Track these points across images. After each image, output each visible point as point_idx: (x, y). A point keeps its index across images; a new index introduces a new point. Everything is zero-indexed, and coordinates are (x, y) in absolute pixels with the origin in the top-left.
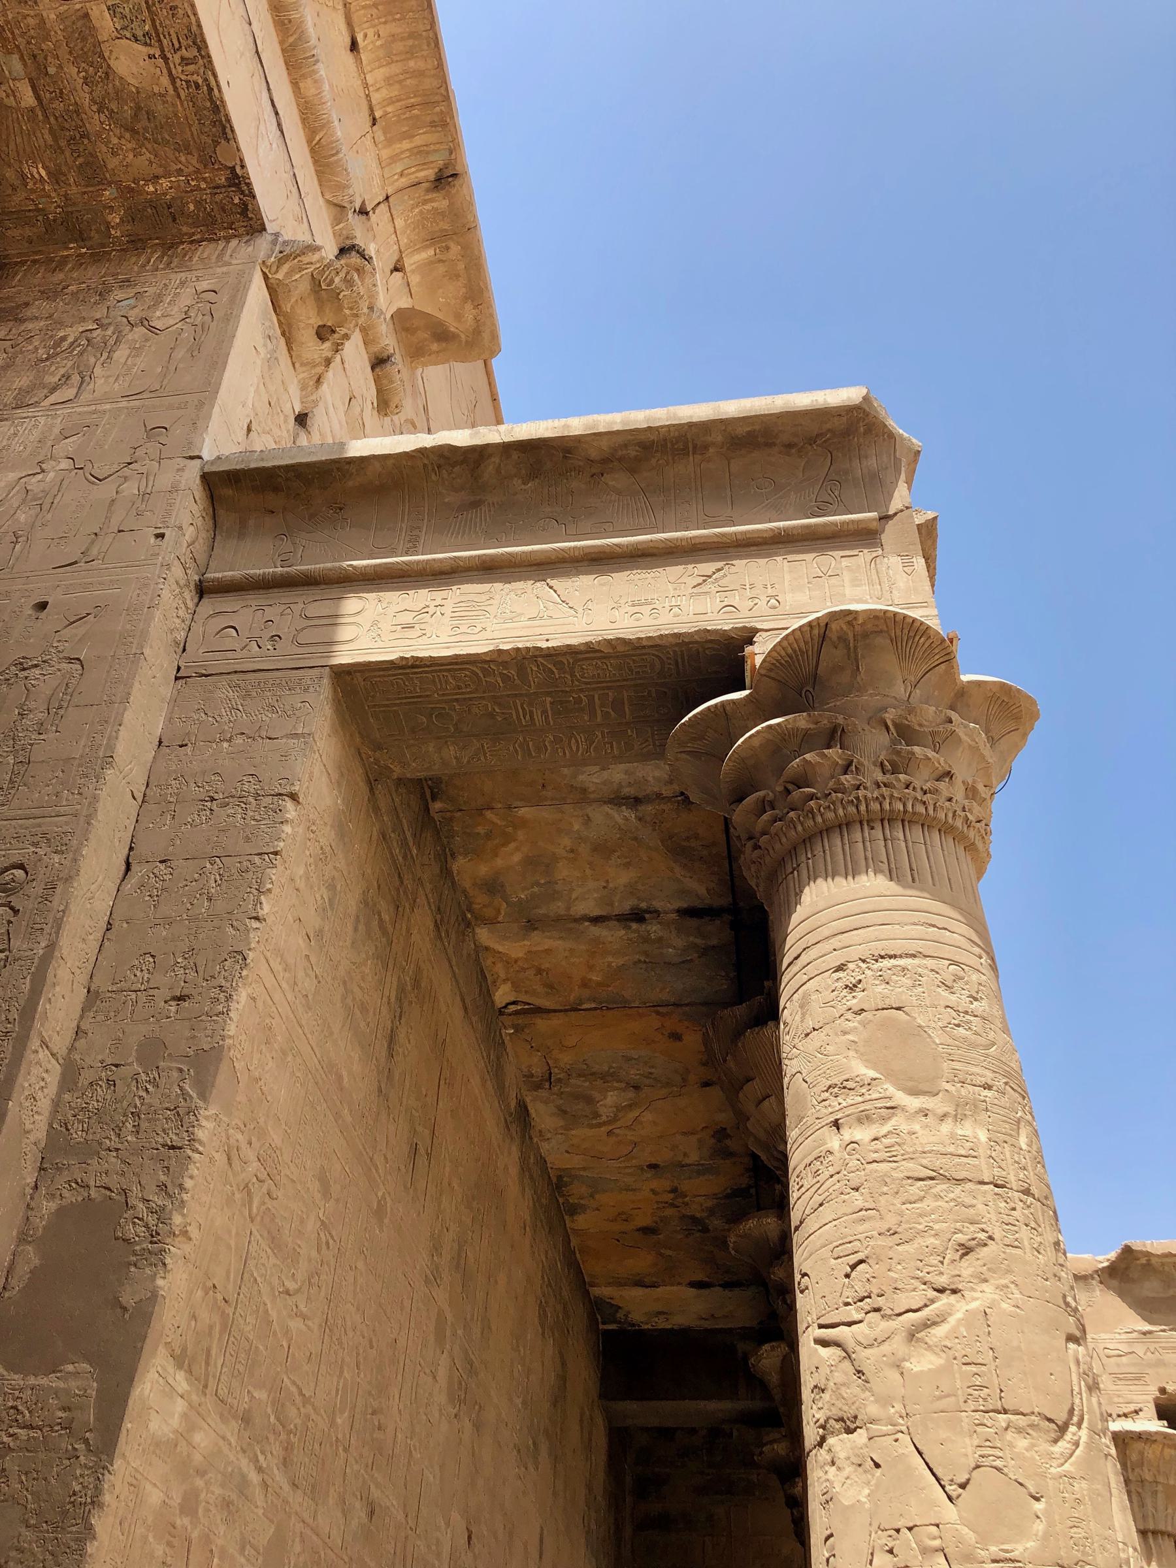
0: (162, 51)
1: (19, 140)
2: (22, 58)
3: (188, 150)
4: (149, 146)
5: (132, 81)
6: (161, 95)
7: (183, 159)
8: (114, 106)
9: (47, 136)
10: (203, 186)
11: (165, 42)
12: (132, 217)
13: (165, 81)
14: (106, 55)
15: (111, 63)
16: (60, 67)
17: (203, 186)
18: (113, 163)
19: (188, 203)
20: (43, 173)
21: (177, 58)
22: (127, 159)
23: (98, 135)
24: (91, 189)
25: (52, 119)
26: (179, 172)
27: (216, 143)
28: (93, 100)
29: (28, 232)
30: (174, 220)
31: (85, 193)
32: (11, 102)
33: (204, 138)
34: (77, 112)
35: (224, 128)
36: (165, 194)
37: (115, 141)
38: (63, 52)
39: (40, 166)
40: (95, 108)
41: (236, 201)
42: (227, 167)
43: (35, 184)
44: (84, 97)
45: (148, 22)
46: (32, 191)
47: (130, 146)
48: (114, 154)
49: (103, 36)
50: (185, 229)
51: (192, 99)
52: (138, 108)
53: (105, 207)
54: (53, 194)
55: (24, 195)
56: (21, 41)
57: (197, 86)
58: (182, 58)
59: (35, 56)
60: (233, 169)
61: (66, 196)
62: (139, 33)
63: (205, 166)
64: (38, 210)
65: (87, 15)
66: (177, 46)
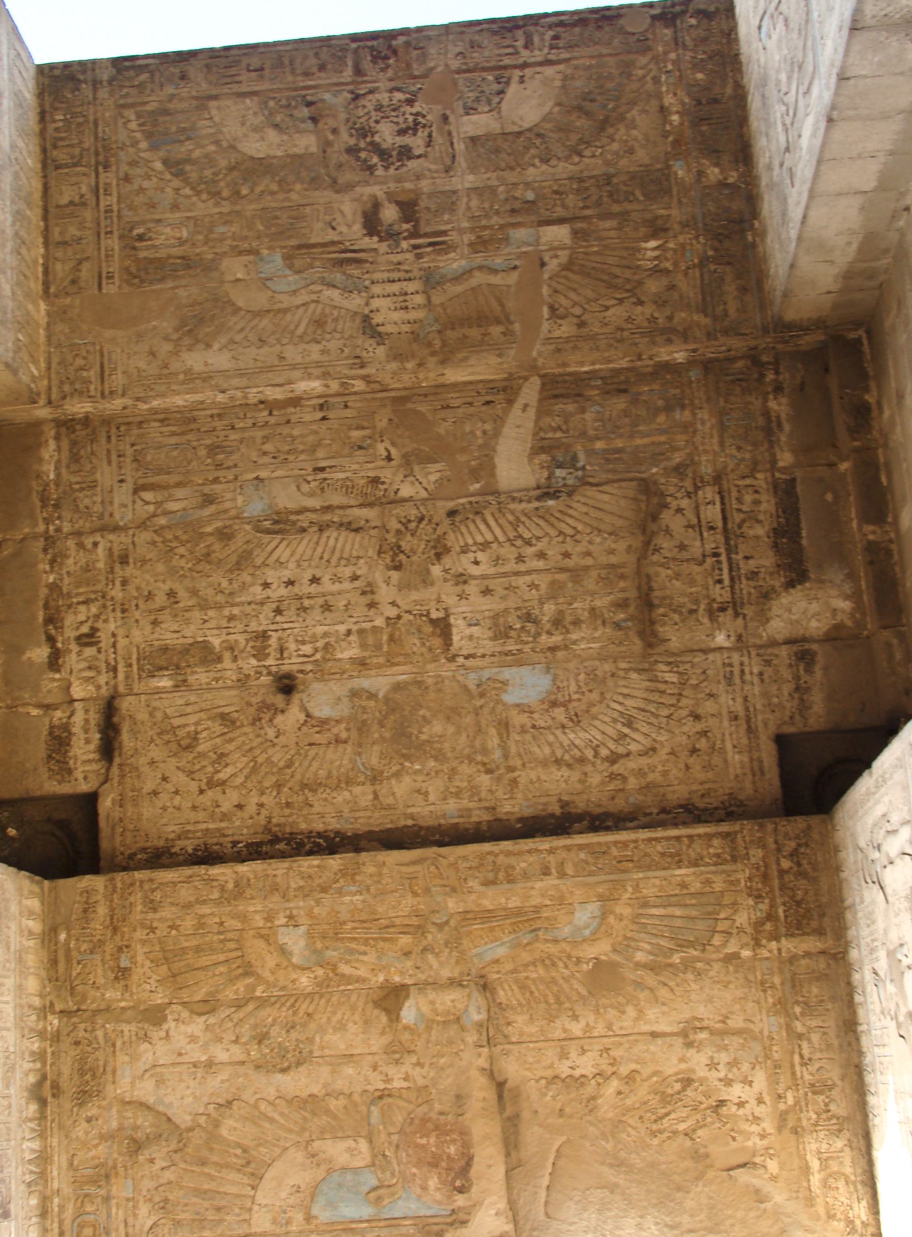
0: (515, 67)
1: (610, 260)
2: (514, 225)
3: (630, 65)
4: (622, 109)
5: (546, 109)
6: (565, 79)
7: (640, 72)
8: (574, 137)
9: (608, 224)
10: (673, 56)
11: (507, 61)
12: (713, 153)
13: (549, 71)
14: (516, 129)
15: (526, 125)
16: (527, 184)
17: (673, 56)
18: (642, 155)
19: (695, 80)
20: (653, 244)
21: (525, 53)
22: (637, 140)
23: (608, 163)
24: (675, 192)
25: (588, 212)
26: (656, 80)
27: (623, 31)
28: (567, 158)
29: (731, 288)
30: (716, 101)
31: (680, 202)
32: (564, 255)
33: (616, 42)
34: (581, 180)
35: (605, 18)
36: (683, 103)
37: (615, 146)
38: (511, 177)
39: (644, 245)
40: (576, 159)
41: (693, 21)
42: (652, 25)
43: (667, 260)
44: (563, 169)
45: (484, 74)
46: (676, 264)
47: (622, 130)
48: (631, 151)
49: (495, 127)
50: (729, 91)
51: (570, 47)
52: (579, 108)
53: (699, 181)
54: (681, 239)
55: (680, 276)
56: (495, 220)
57: (556, 38)
58: (526, 47)
59: (513, 211)
60: (654, 18)
61: (685, 225)
62: (496, 87)
63: (649, 49)
64: (701, 265)
65: (473, 140)
66: (510, 50)
